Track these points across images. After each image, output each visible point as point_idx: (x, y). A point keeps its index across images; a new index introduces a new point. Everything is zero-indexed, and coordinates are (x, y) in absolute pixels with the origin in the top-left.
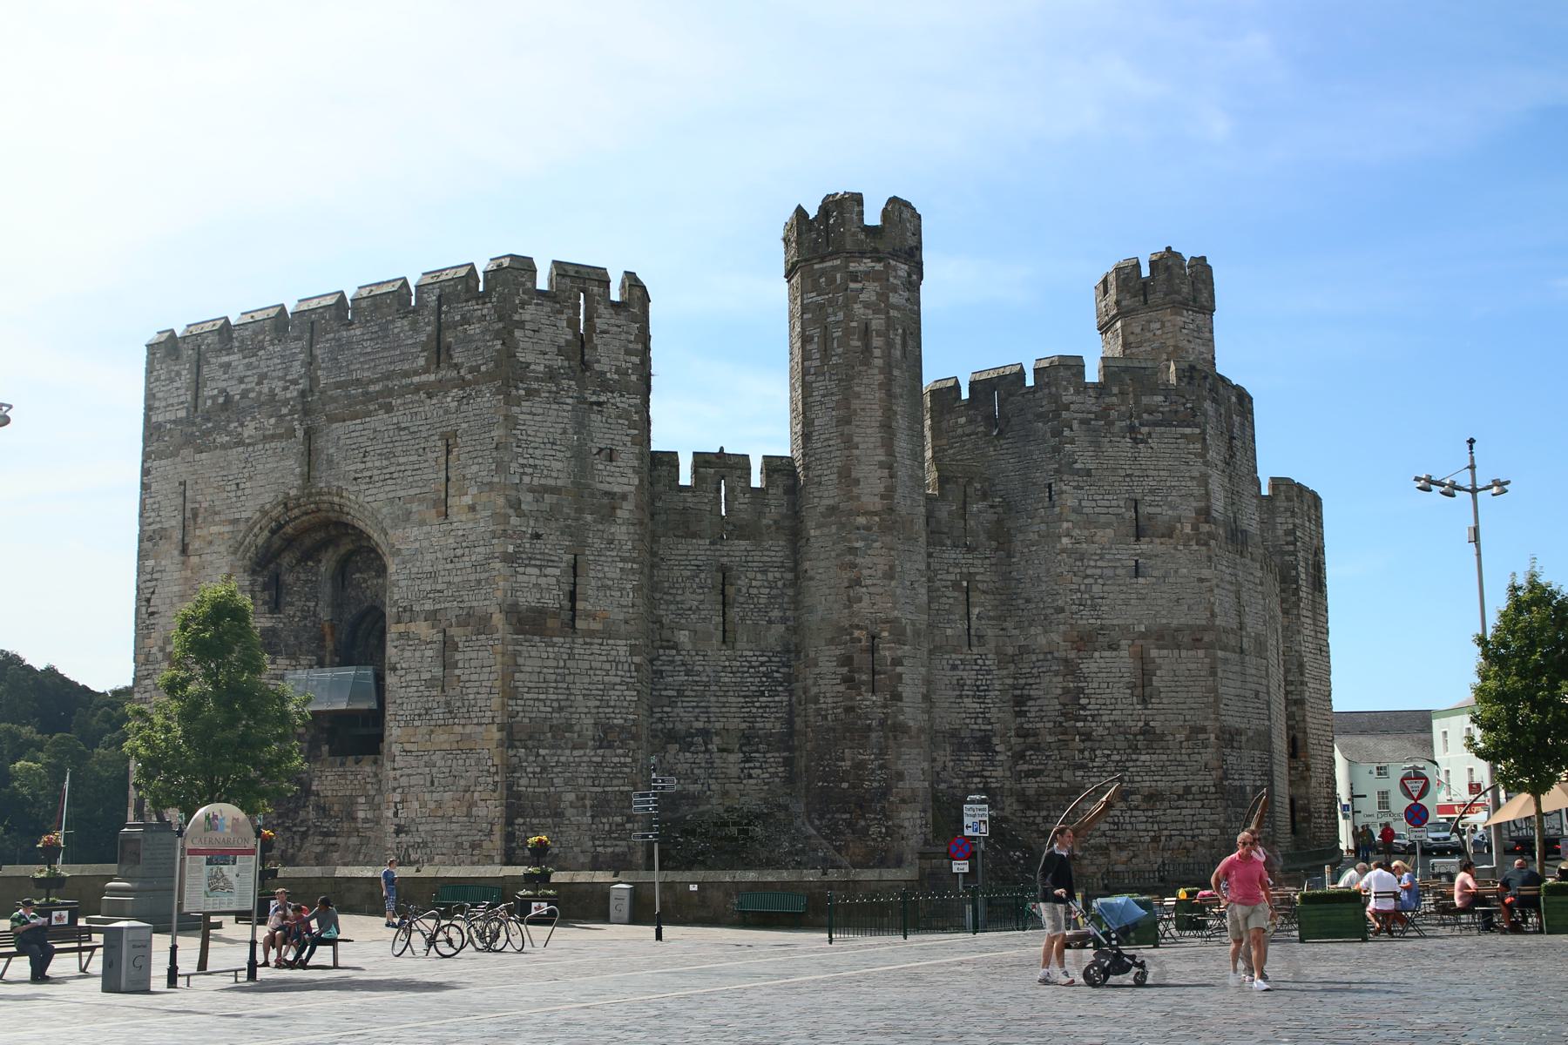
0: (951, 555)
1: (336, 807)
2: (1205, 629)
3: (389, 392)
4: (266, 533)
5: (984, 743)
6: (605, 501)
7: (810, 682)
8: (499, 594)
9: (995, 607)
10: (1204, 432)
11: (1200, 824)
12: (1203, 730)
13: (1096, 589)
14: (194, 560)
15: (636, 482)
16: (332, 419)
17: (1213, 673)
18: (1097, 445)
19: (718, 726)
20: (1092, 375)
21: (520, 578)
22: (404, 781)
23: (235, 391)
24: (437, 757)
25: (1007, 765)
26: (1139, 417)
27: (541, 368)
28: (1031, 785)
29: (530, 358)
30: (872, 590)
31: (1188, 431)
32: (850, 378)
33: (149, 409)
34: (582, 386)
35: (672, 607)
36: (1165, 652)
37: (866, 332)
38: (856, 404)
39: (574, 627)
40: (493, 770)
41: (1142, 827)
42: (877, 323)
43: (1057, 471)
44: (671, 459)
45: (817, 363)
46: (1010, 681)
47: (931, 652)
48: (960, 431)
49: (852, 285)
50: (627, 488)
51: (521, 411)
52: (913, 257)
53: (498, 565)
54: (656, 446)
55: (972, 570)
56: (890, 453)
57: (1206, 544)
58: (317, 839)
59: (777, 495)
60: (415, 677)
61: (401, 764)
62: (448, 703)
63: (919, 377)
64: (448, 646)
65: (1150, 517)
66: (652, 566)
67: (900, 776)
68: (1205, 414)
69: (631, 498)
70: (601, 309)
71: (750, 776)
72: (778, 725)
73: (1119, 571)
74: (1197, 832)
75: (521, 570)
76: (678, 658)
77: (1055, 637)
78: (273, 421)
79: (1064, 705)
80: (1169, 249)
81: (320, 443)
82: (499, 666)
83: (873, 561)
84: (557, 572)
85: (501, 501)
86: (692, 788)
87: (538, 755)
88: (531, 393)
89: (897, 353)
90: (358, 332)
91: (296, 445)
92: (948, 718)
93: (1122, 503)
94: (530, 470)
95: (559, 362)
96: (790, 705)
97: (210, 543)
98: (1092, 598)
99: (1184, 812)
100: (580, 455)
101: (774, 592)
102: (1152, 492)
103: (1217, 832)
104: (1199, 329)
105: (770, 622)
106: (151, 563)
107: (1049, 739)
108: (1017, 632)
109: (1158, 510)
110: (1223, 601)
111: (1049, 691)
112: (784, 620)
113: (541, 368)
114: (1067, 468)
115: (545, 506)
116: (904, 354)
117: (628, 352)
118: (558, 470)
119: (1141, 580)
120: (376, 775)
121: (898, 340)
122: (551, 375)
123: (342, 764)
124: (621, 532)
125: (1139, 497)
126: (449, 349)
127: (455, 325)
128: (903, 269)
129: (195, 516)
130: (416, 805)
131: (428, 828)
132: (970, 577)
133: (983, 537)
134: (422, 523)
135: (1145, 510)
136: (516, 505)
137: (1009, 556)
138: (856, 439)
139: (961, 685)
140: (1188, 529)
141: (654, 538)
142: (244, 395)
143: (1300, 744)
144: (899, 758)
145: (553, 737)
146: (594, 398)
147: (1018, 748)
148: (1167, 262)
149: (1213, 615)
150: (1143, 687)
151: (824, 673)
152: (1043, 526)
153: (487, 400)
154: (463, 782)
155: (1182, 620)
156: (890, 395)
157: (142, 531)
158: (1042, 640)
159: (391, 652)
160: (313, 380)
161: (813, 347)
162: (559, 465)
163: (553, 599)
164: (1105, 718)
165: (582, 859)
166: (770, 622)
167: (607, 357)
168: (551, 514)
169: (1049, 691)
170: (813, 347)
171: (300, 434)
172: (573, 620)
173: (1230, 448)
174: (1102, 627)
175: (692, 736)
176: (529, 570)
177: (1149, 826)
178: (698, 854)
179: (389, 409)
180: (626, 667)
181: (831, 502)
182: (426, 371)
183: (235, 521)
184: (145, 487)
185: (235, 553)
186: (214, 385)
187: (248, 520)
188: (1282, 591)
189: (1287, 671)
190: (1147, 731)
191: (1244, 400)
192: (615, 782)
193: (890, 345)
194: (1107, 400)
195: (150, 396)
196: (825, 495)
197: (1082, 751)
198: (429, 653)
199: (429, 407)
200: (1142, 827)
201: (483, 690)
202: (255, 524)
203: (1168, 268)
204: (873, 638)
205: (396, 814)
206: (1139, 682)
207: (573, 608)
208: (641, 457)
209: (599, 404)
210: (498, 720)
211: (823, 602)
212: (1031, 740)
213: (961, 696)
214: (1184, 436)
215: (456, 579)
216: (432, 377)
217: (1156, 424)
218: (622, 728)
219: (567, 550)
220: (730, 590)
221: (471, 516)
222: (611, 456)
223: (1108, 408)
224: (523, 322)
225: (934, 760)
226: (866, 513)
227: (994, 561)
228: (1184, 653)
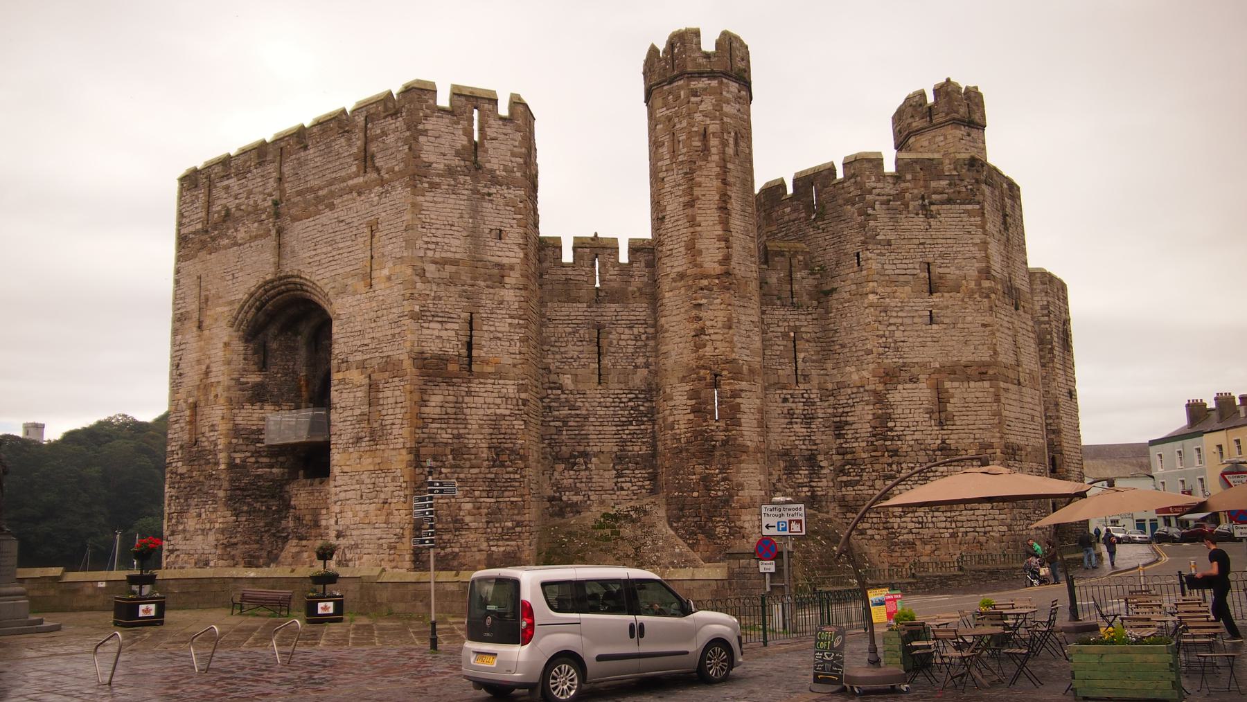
0: (779, 312)
1: (308, 517)
2: (988, 365)
3: (332, 194)
5: (811, 460)
6: (496, 271)
7: (667, 412)
8: (408, 344)
9: (818, 353)
10: (982, 208)
11: (990, 523)
12: (991, 446)
13: (898, 334)
14: (206, 333)
15: (522, 255)
16: (295, 219)
17: (998, 400)
18: (894, 220)
19: (596, 449)
20: (889, 167)
21: (425, 331)
22: (342, 496)
24: (365, 476)
25: (830, 477)
26: (929, 197)
27: (442, 166)
28: (849, 492)
29: (432, 158)
30: (713, 337)
31: (969, 207)
32: (692, 171)
33: (180, 224)
34: (475, 179)
35: (558, 356)
36: (956, 384)
37: (705, 135)
38: (697, 192)
39: (470, 370)
40: (404, 485)
41: (943, 525)
42: (714, 127)
43: (864, 242)
44: (555, 244)
45: (668, 162)
46: (830, 411)
47: (766, 389)
48: (786, 218)
49: (693, 99)
50: (514, 261)
51: (426, 200)
52: (743, 80)
53: (406, 321)
54: (545, 231)
55: (798, 323)
56: (727, 230)
57: (988, 297)
58: (295, 542)
59: (640, 266)
60: (350, 413)
63: (750, 172)
64: (373, 387)
65: (941, 276)
66: (541, 326)
67: (740, 486)
68: (983, 195)
69: (517, 268)
70: (491, 121)
71: (622, 489)
72: (644, 448)
73: (916, 320)
74: (988, 529)
75: (426, 325)
76: (563, 396)
77: (865, 373)
78: (256, 225)
79: (874, 428)
80: (948, 80)
81: (286, 238)
82: (408, 403)
83: (714, 315)
84: (456, 326)
85: (409, 271)
86: (575, 498)
87: (441, 473)
88: (433, 186)
89: (730, 150)
90: (311, 151)
91: (270, 242)
92: (779, 437)
93: (917, 266)
94: (432, 246)
95: (457, 162)
96: (653, 432)
97: (216, 320)
98: (896, 342)
99: (977, 512)
100: (474, 235)
101: (639, 343)
102: (942, 256)
103: (1005, 528)
104: (974, 141)
105: (636, 367)
106: (179, 337)
107: (864, 455)
108: (835, 372)
109: (947, 270)
110: (1005, 345)
111: (862, 417)
112: (647, 365)
113: (442, 166)
114: (870, 239)
115: (445, 274)
116: (736, 154)
117: (513, 155)
118: (457, 246)
119: (934, 326)
121: (731, 141)
122: (451, 172)
123: (311, 485)
124: (509, 295)
125: (931, 260)
126: (373, 156)
127: (377, 137)
128: (734, 87)
129: (207, 300)
130: (350, 514)
132: (796, 329)
133: (805, 298)
134: (355, 293)
135: (936, 271)
136: (422, 274)
137: (827, 312)
138: (698, 219)
139: (791, 413)
140: (972, 285)
141: (542, 303)
142: (238, 208)
143: (1058, 462)
144: (738, 472)
145: (454, 459)
146: (486, 190)
147: (838, 464)
148: (946, 90)
149: (995, 352)
150: (940, 412)
151: (677, 408)
152: (854, 287)
153: (400, 193)
154: (382, 496)
155: (971, 358)
156: (725, 182)
157: (175, 315)
158: (855, 377)
159: (334, 394)
160: (283, 191)
161: (664, 150)
162: (457, 242)
163: (453, 347)
164: (908, 438)
165: (478, 556)
166: (636, 367)
167: (497, 158)
168: (451, 281)
169: (862, 417)
170: (664, 150)
171: (273, 232)
172: (470, 365)
173: (1005, 223)
174: (904, 365)
175: (575, 457)
176: (432, 325)
177: (948, 525)
178: (579, 551)
179: (331, 207)
180: (514, 402)
181: (680, 269)
182: (357, 175)
183: (231, 303)
184: (177, 282)
185: (232, 326)
186: (219, 202)
188: (1041, 350)
189: (1046, 409)
190: (944, 448)
191: (1012, 190)
192: (506, 494)
193: (724, 144)
194: (903, 185)
195: (181, 215)
196: (675, 263)
197: (890, 465)
198: (359, 394)
199: (360, 204)
200: (943, 525)
201: (397, 421)
202: (246, 302)
203: (947, 94)
204: (716, 375)
205: (337, 522)
206: (936, 408)
207: (470, 356)
208: (526, 236)
209: (489, 195)
210: (408, 445)
211: (677, 350)
212: (849, 456)
213: (791, 423)
214: (966, 211)
215: (378, 335)
216: (361, 180)
217: (942, 203)
218: (512, 451)
219: (464, 309)
220: (604, 343)
221: (388, 285)
222: (500, 235)
223: (904, 191)
224: (426, 130)
225: (771, 474)
226: (707, 277)
227: (814, 316)
228: (972, 384)
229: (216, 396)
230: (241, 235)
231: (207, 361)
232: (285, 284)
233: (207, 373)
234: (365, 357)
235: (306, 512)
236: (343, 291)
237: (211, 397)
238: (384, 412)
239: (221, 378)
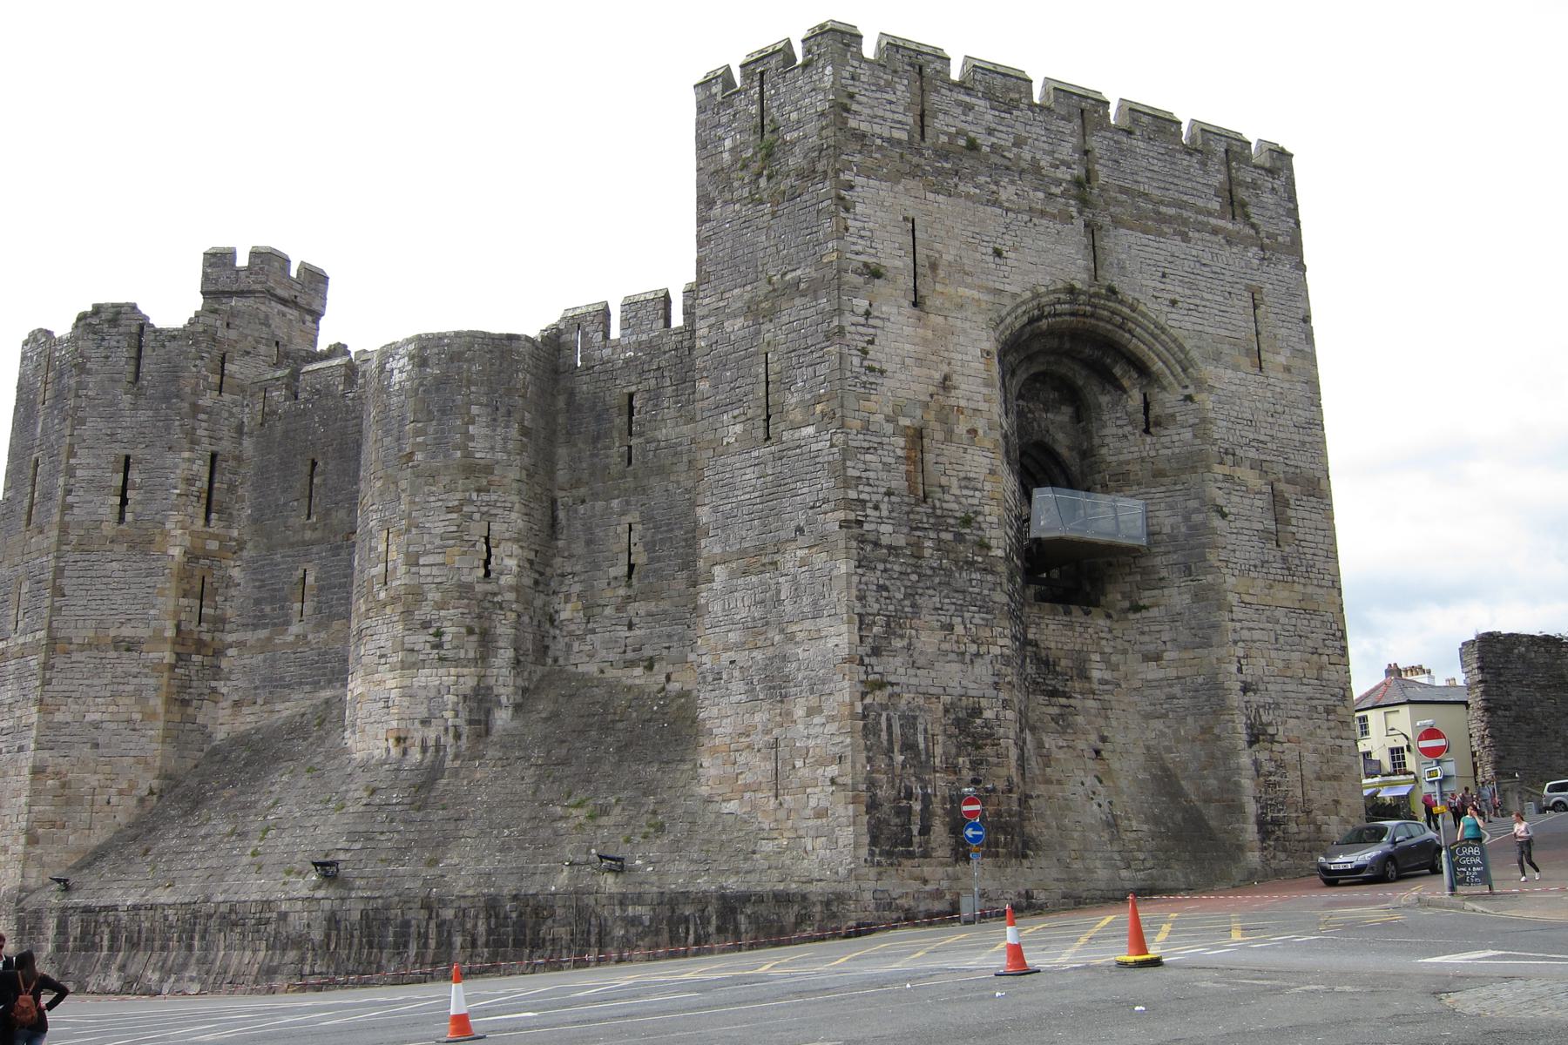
1: (1063, 662)
3: (1185, 222)
4: (1025, 319)
14: (936, 320)
16: (1117, 222)
22: (1246, 634)
23: (985, 142)
61: (1241, 616)
62: (1284, 559)
78: (1041, 195)
81: (1106, 243)
120: (1110, 631)
123: (1068, 613)
129: (934, 267)
131: (1278, 687)
134: (1236, 368)
160: (1089, 176)
171: (1079, 223)
179: (1185, 238)
187: (1014, 296)
202: (1023, 303)
205: (1240, 670)
229: (973, 432)
230: (1007, 193)
231: (945, 369)
232: (1094, 306)
233: (946, 384)
234: (1263, 457)
235: (1061, 654)
236: (1217, 357)
237: (961, 429)
238: (1299, 536)
239: (983, 406)
